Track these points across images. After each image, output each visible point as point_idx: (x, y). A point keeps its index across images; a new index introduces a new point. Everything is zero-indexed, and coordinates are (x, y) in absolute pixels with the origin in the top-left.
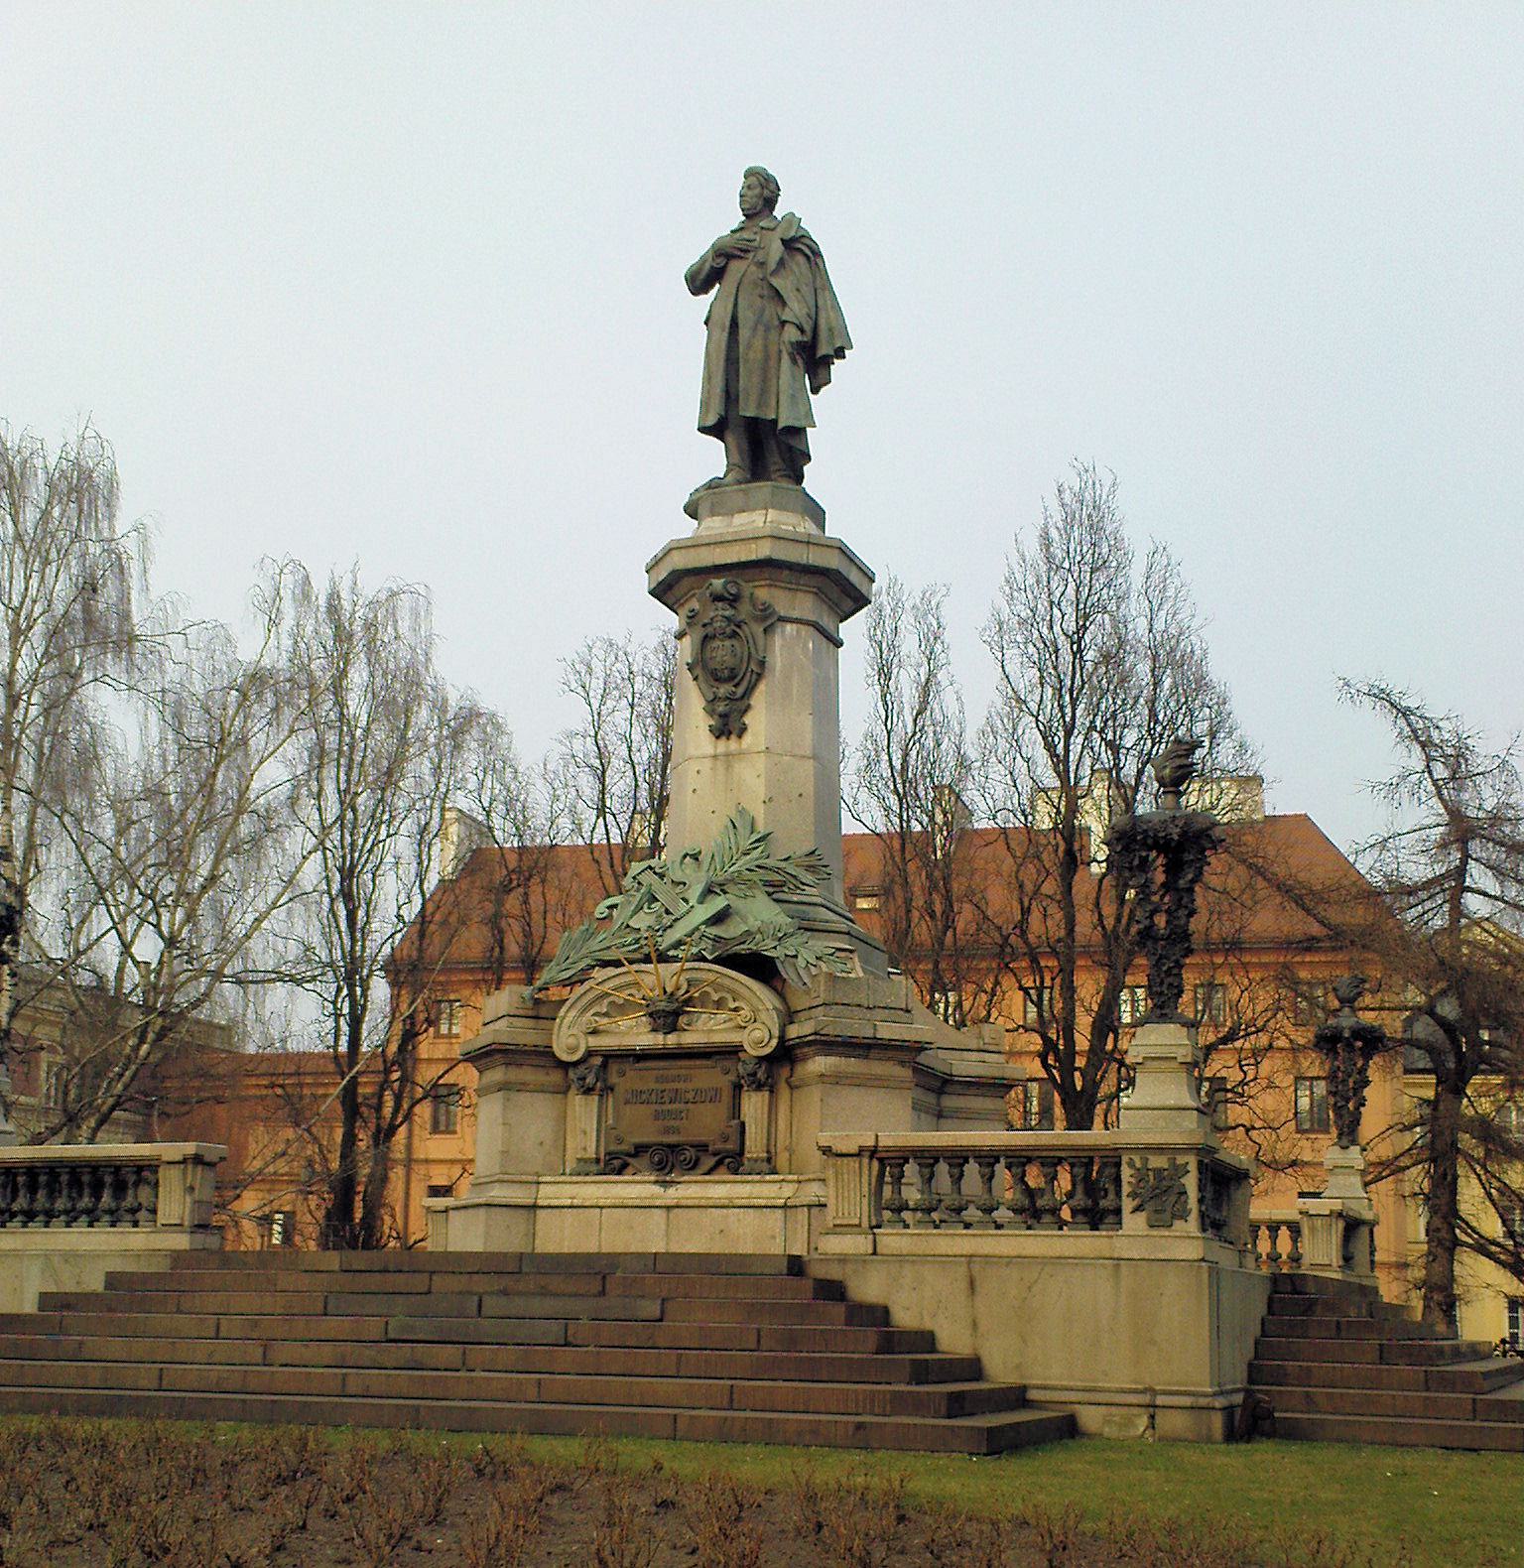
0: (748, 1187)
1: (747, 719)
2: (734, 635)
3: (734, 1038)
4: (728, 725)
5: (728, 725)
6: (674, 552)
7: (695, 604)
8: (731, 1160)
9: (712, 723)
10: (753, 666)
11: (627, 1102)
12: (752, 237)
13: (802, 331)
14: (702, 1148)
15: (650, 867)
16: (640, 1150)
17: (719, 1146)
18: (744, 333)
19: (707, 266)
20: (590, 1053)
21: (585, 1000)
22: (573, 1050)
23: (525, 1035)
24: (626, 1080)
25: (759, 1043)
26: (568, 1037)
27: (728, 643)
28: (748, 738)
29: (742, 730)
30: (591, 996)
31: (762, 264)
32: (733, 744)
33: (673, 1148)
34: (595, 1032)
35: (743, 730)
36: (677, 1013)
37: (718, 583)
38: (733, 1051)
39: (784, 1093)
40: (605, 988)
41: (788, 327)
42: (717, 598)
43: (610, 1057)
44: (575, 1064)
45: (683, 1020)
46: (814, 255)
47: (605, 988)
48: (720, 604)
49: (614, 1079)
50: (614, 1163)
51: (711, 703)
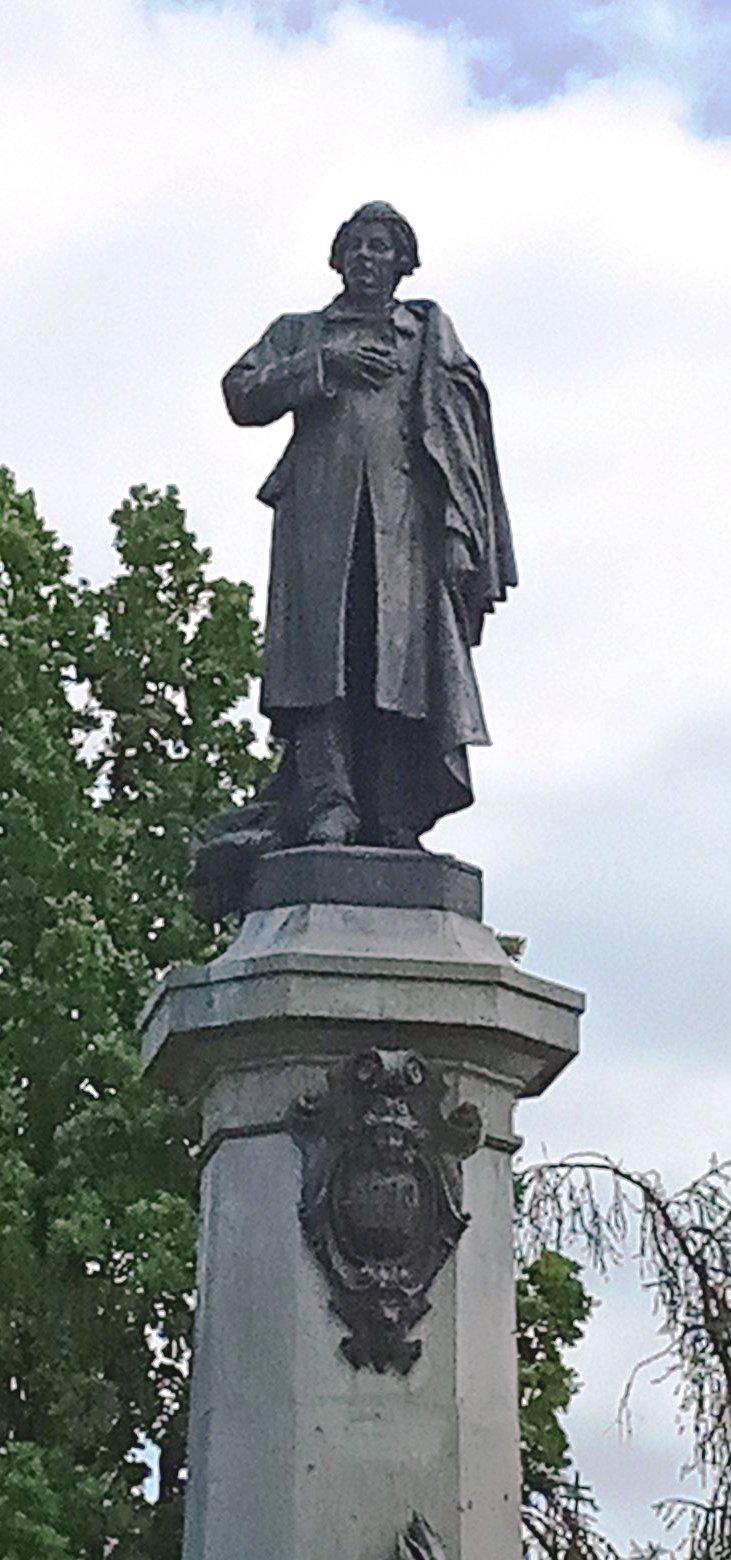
1: (419, 1333)
2: (417, 1168)
4: (379, 1340)
5: (379, 1340)
6: (295, 981)
9: (347, 1334)
12: (381, 347)
13: (472, 547)
19: (306, 386)
27: (404, 1180)
28: (421, 1370)
32: (390, 1380)
35: (415, 1352)
42: (396, 1086)
46: (477, 398)
48: (389, 1102)
51: (347, 1304)
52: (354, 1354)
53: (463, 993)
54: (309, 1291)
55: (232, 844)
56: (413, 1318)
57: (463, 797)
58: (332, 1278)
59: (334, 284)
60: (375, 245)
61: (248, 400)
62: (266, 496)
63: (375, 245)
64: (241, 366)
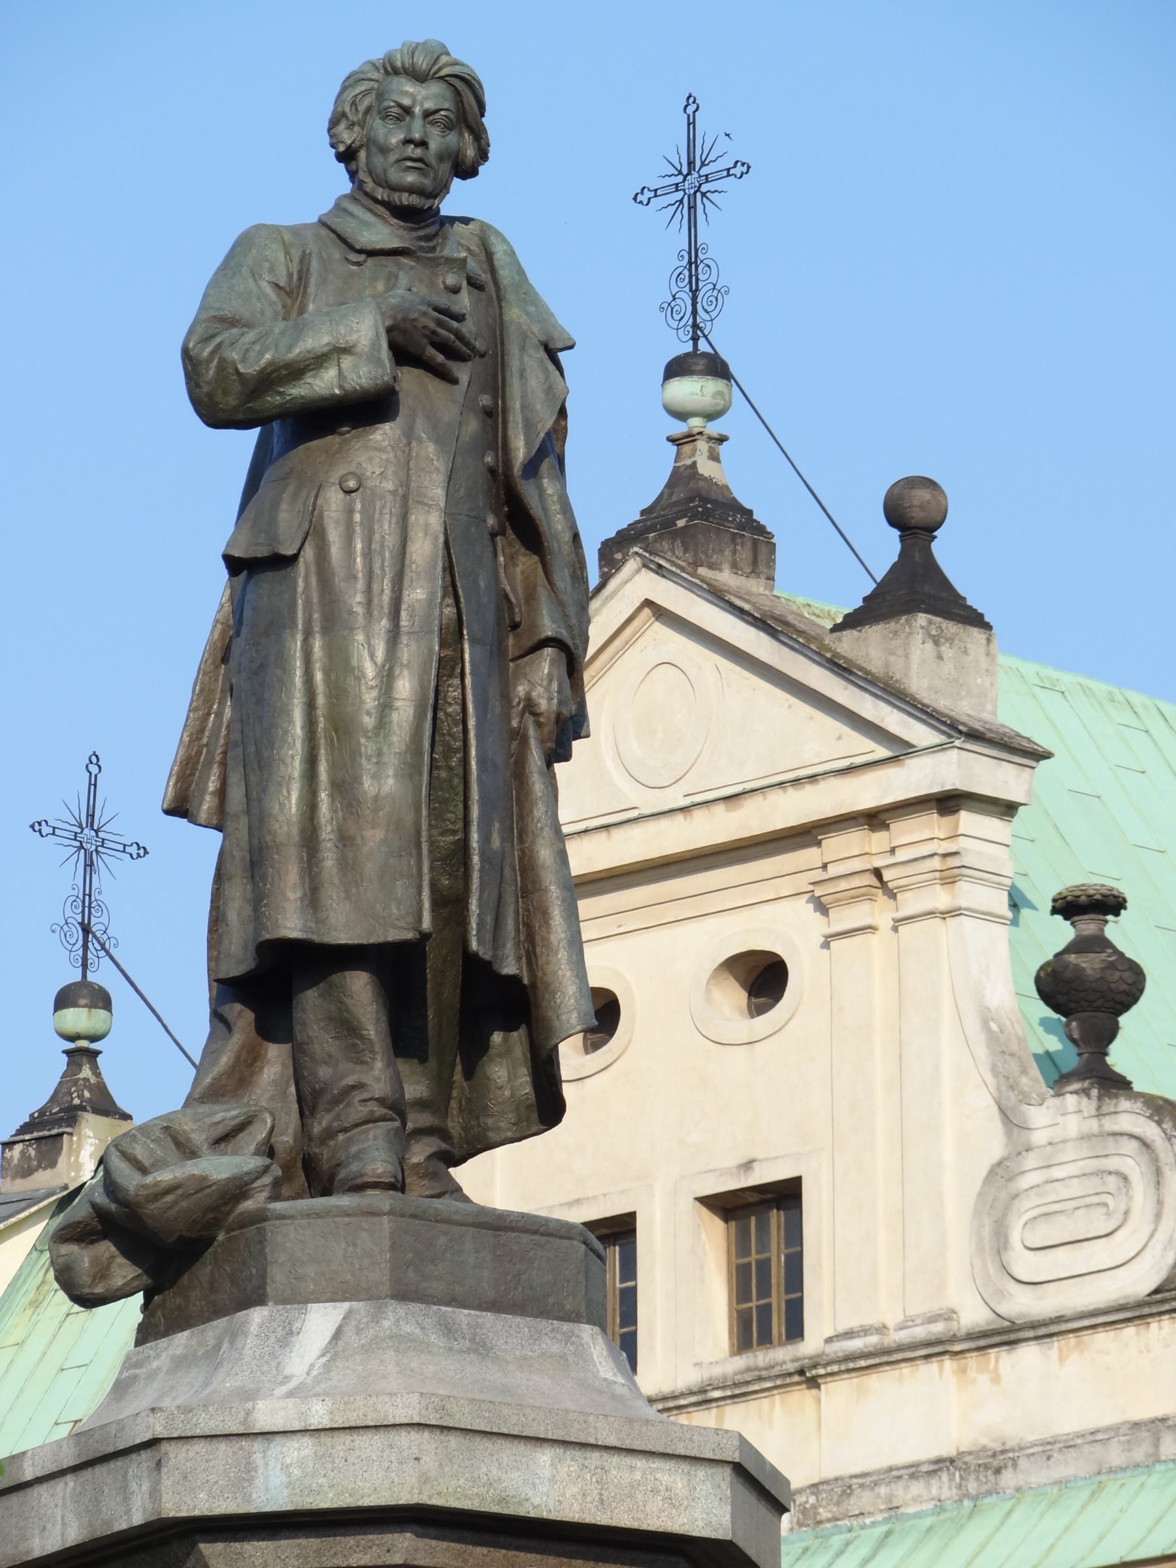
55: (202, 1183)
59: (339, 181)
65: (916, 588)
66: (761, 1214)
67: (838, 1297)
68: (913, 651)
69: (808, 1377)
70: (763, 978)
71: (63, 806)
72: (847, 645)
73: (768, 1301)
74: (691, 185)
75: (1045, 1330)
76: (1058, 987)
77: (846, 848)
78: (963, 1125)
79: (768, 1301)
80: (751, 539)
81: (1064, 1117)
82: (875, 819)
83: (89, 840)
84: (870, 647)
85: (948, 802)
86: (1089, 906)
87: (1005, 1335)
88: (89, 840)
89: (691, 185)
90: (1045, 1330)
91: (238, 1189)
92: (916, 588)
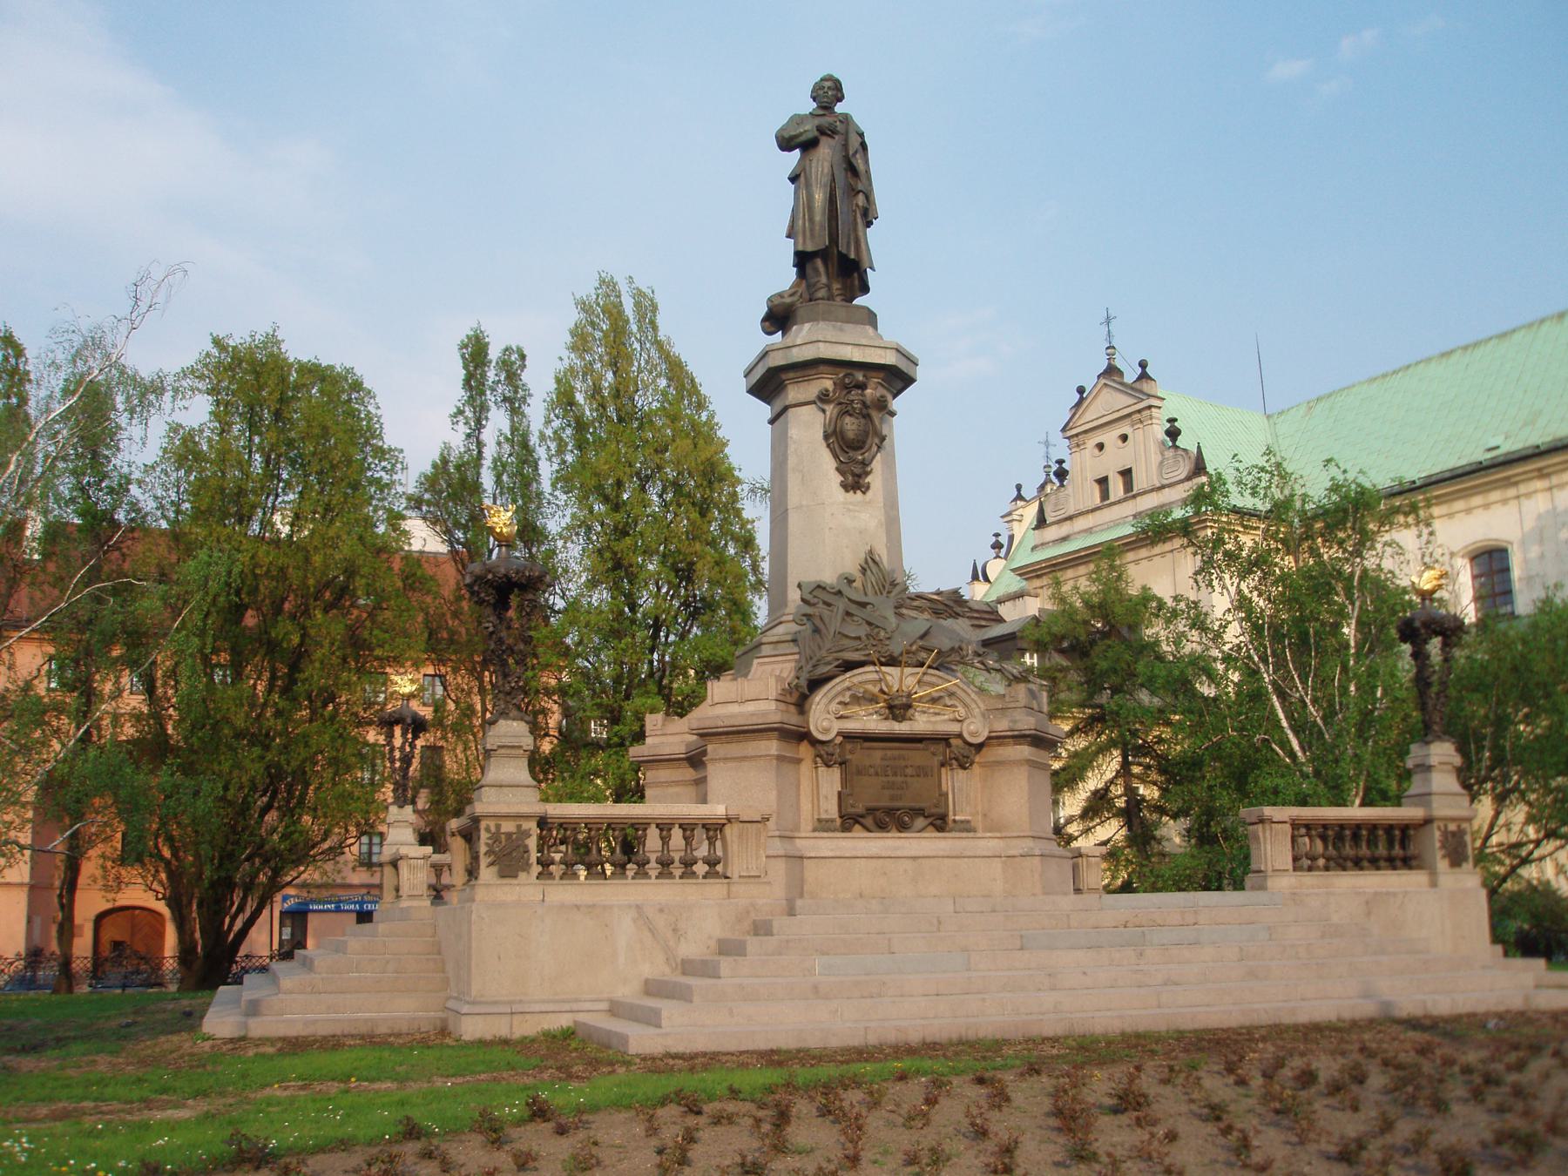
0: (964, 842)
3: (954, 728)
5: (855, 481)
7: (828, 384)
8: (940, 823)
10: (877, 440)
11: (859, 773)
14: (920, 812)
15: (819, 586)
16: (871, 811)
17: (934, 810)
18: (838, 193)
20: (839, 734)
21: (834, 692)
22: (827, 731)
23: (793, 719)
24: (858, 756)
25: (972, 734)
26: (824, 717)
28: (870, 494)
29: (865, 489)
30: (839, 688)
31: (845, 146)
33: (890, 811)
34: (841, 717)
35: (868, 488)
36: (909, 706)
37: (860, 377)
38: (943, 740)
39: (976, 768)
40: (855, 680)
41: (861, 197)
43: (849, 737)
44: (823, 743)
45: (911, 711)
47: (855, 680)
49: (849, 757)
50: (849, 821)
52: (846, 487)
53: (879, 351)
54: (827, 462)
56: (867, 474)
57: (865, 289)
58: (836, 456)
60: (829, 92)
61: (786, 144)
62: (794, 179)
63: (829, 92)
64: (782, 129)
65: (1144, 376)
66: (1126, 474)
67: (1140, 482)
68: (1146, 387)
69: (1134, 497)
70: (1124, 438)
71: (1043, 438)
72: (1137, 385)
73: (1128, 486)
74: (1108, 321)
75: (1170, 485)
76: (1168, 433)
77: (1137, 416)
78: (1155, 458)
79: (1128, 486)
80: (1121, 373)
81: (1170, 454)
82: (1139, 411)
83: (1047, 444)
84: (1137, 385)
85: (1150, 407)
86: (1172, 421)
87: (1163, 487)
88: (1047, 444)
89: (1108, 321)
90: (1170, 485)
91: (792, 305)
92: (1144, 376)
